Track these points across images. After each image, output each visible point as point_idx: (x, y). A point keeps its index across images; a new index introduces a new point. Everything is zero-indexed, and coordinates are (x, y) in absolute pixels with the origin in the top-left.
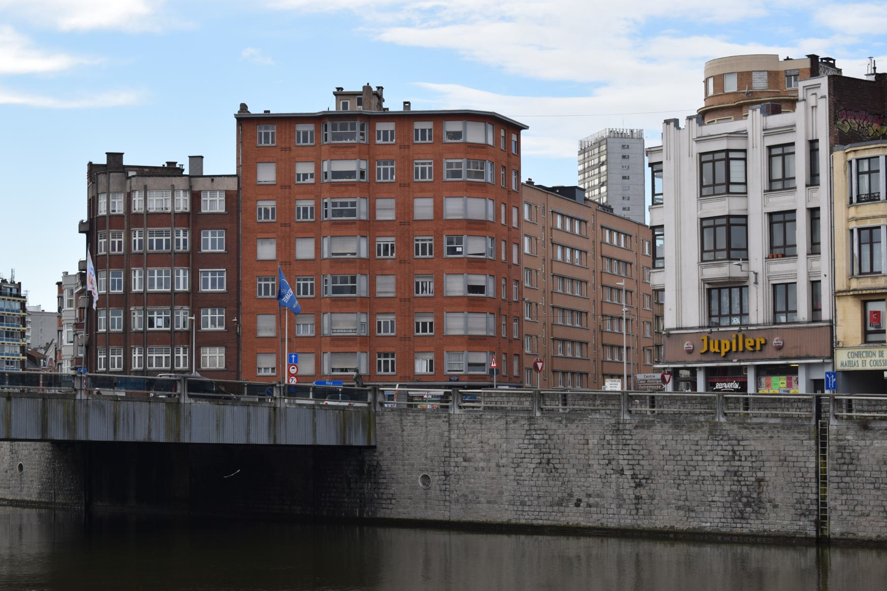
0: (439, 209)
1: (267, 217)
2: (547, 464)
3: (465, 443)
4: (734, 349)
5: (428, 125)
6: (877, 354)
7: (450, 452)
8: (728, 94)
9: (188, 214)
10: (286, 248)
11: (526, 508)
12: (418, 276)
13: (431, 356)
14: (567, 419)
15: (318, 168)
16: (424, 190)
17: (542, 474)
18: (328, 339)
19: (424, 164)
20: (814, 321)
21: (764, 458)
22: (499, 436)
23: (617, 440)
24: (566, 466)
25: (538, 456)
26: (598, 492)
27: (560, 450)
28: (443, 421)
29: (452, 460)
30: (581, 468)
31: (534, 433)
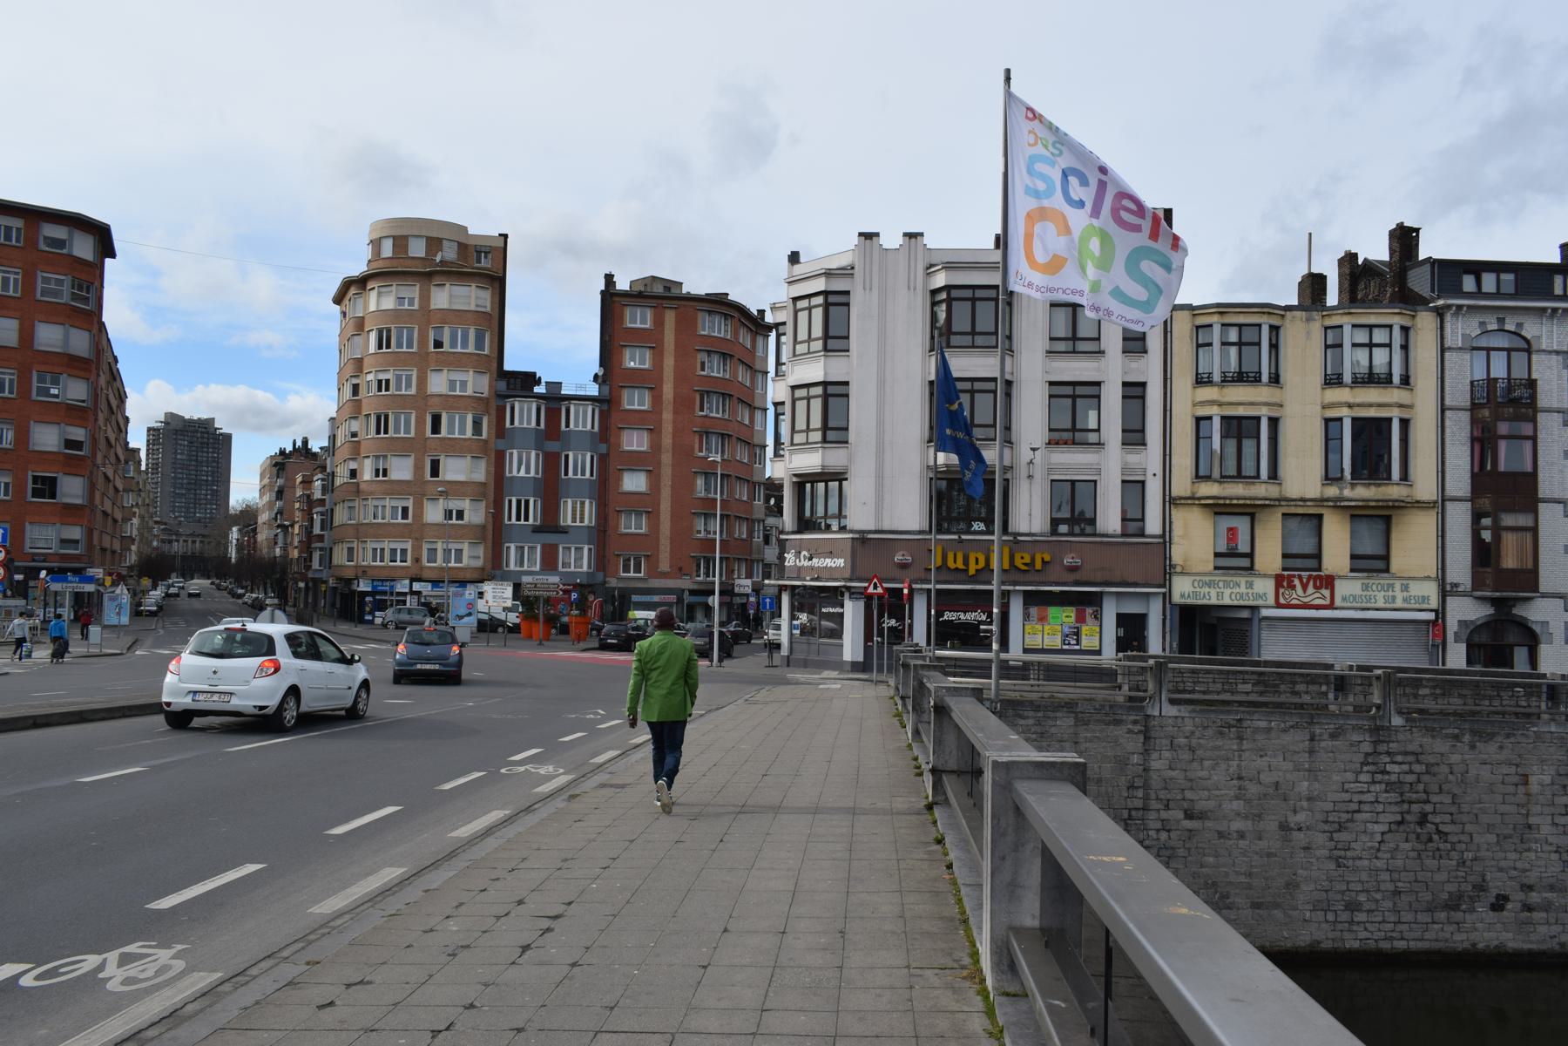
3: (1191, 780)
6: (1243, 585)
7: (1146, 798)
11: (1361, 917)
14: (1474, 732)
17: (1407, 846)
24: (1469, 828)
26: (1552, 880)
27: (1454, 796)
28: (1130, 731)
29: (1153, 815)
31: (1388, 760)
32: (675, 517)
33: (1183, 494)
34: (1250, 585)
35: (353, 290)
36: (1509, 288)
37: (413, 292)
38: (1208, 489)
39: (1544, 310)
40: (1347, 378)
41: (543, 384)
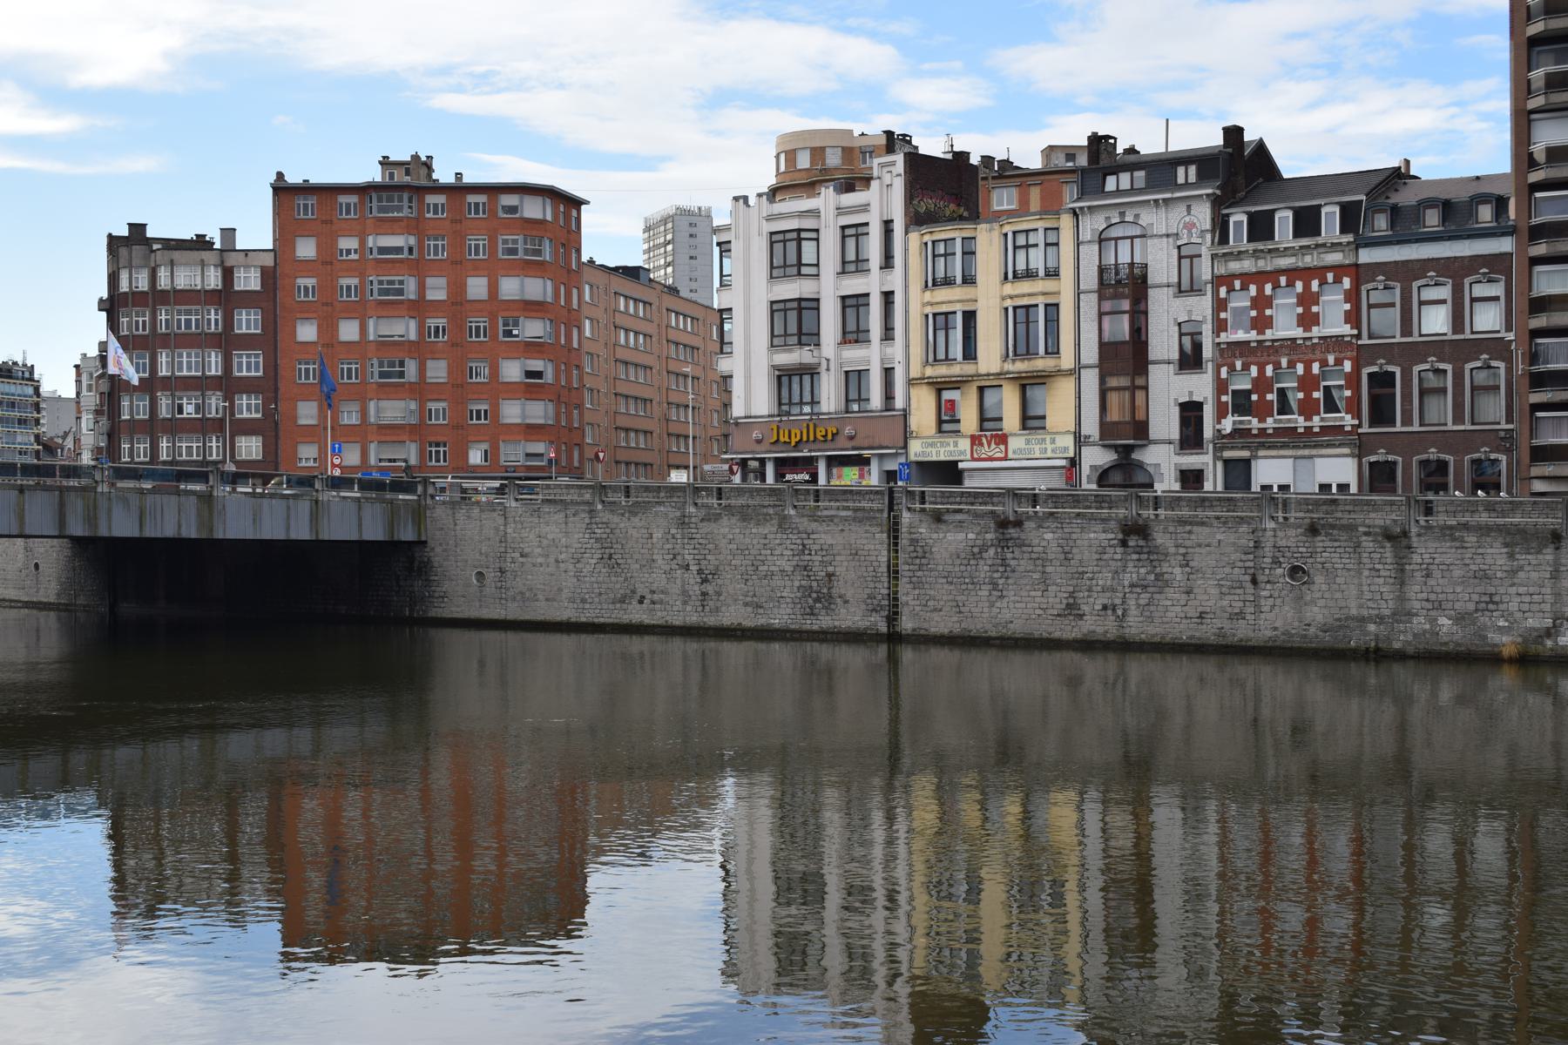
0: (493, 288)
1: (306, 295)
2: (609, 560)
4: (805, 439)
5: (481, 199)
6: (952, 444)
8: (800, 170)
9: (220, 291)
10: (328, 328)
11: (587, 606)
12: (472, 360)
13: (485, 446)
14: (630, 512)
15: (363, 243)
16: (477, 268)
17: (604, 570)
18: (375, 427)
19: (477, 241)
20: (887, 410)
21: (835, 552)
22: (558, 530)
23: (683, 534)
25: (599, 551)
29: (508, 555)
30: (644, 563)
34: (956, 444)
36: (1140, 183)
39: (1149, 201)
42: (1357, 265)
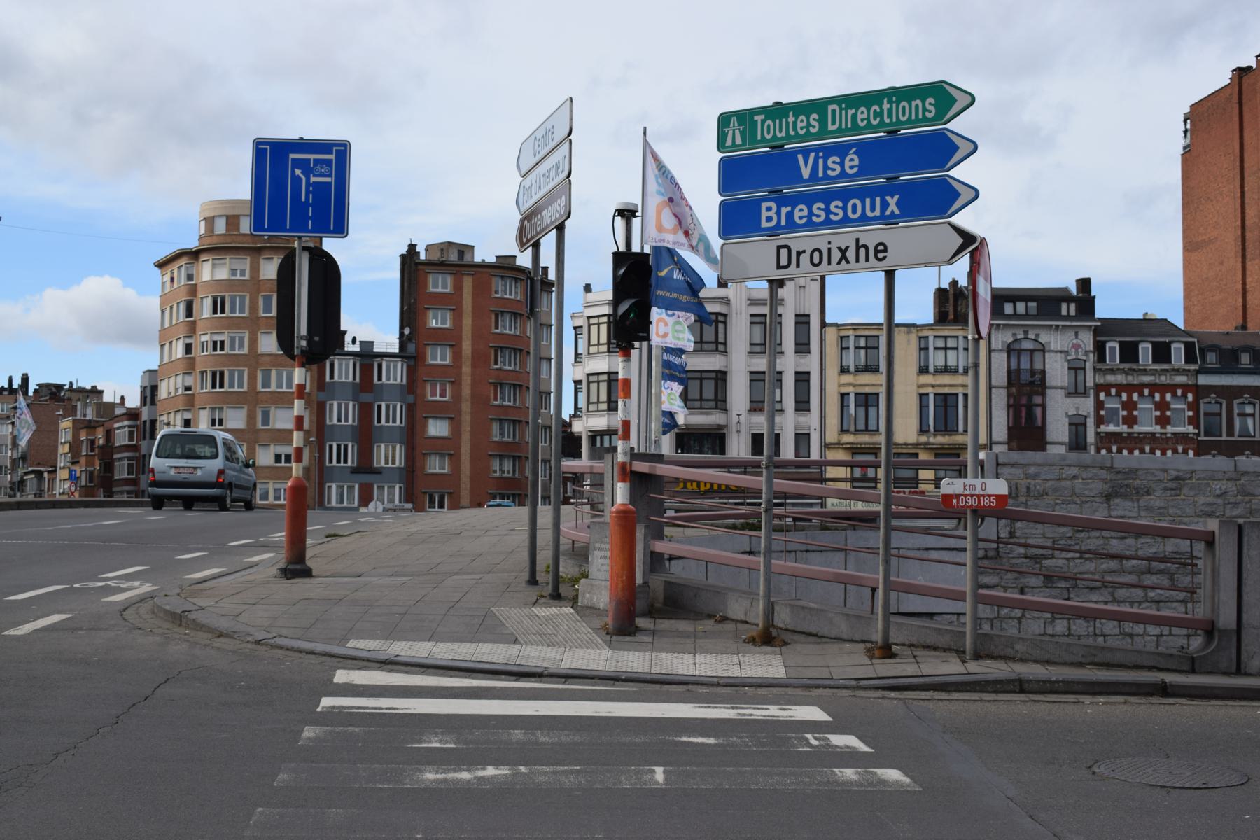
32: (474, 459)
33: (833, 441)
35: (184, 261)
37: (245, 264)
38: (848, 438)
39: (1051, 326)
40: (931, 369)
41: (358, 343)
42: (1197, 386)
